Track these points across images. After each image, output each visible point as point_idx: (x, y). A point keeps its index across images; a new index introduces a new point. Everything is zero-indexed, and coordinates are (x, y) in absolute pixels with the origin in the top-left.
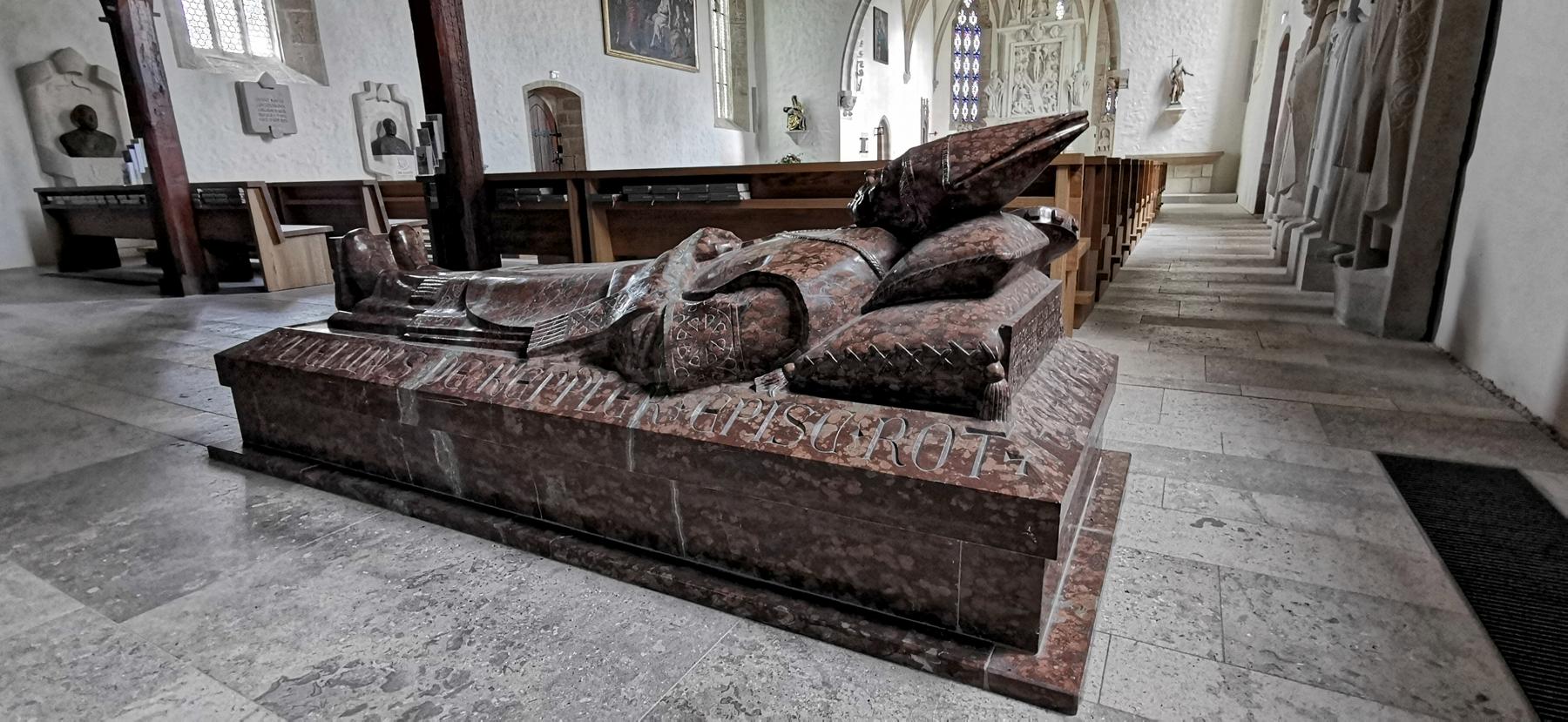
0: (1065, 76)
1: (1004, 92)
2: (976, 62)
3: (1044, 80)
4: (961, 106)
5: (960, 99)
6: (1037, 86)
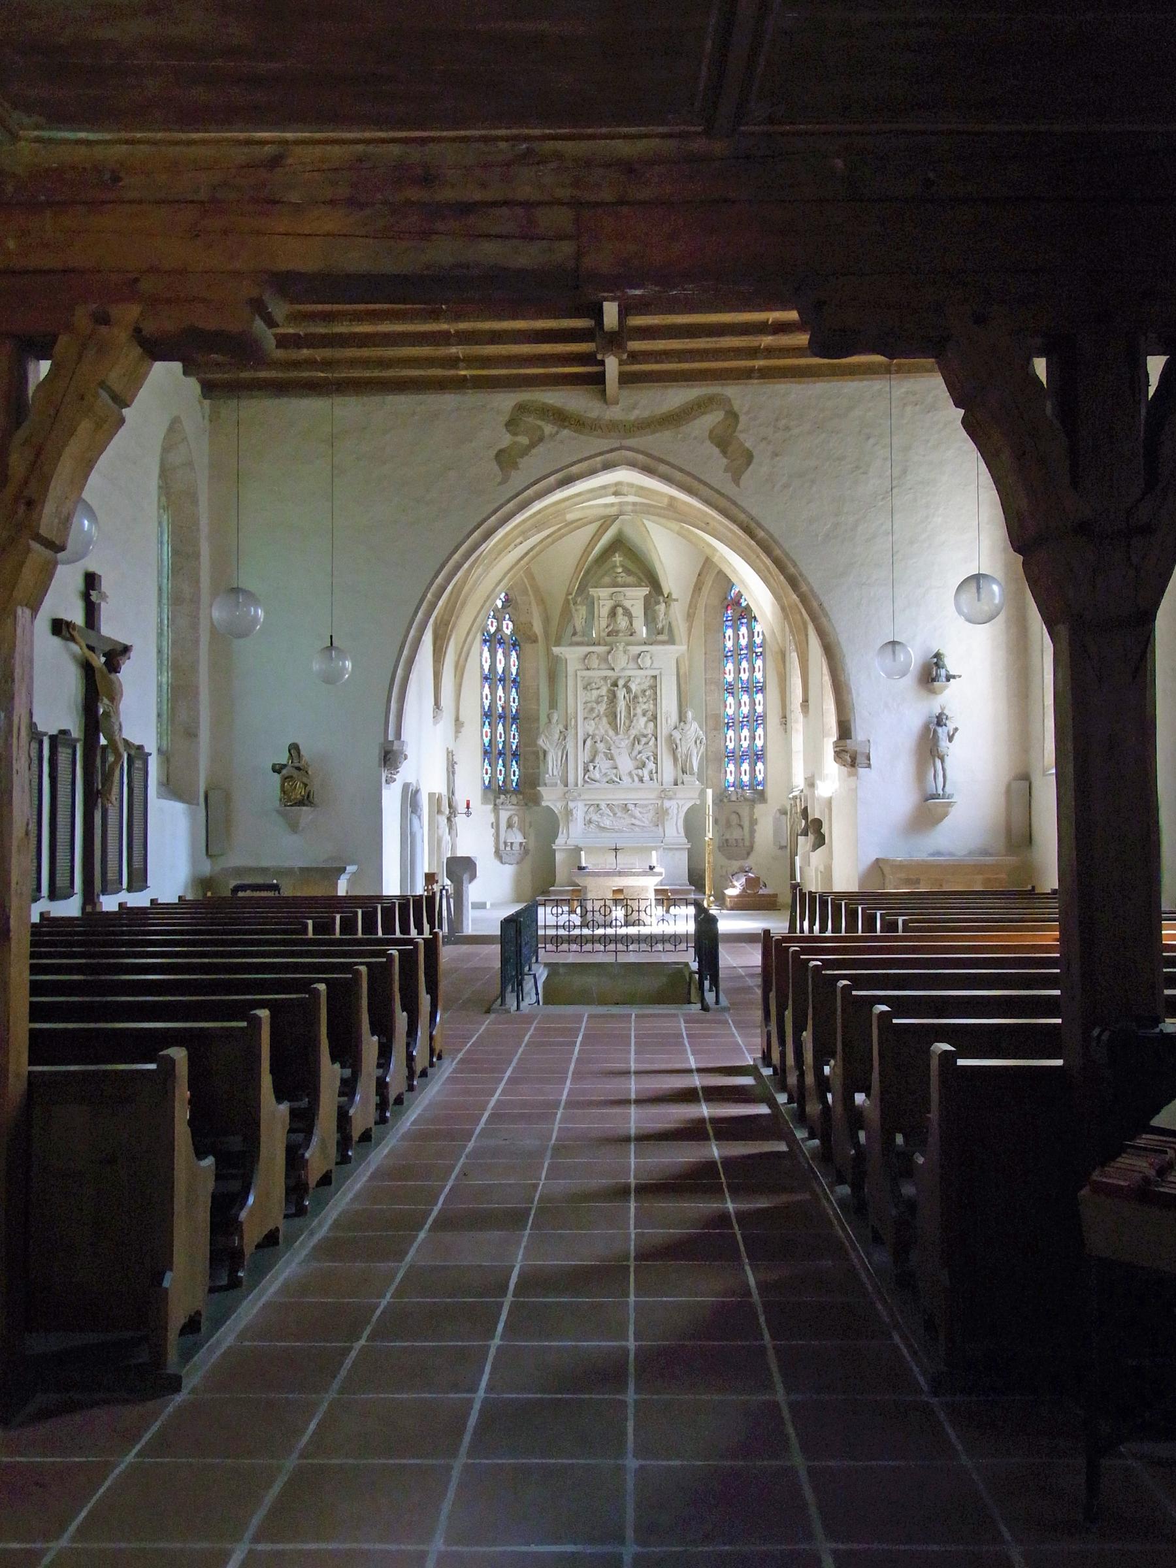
0: (663, 731)
2: (514, 693)
3: (633, 732)
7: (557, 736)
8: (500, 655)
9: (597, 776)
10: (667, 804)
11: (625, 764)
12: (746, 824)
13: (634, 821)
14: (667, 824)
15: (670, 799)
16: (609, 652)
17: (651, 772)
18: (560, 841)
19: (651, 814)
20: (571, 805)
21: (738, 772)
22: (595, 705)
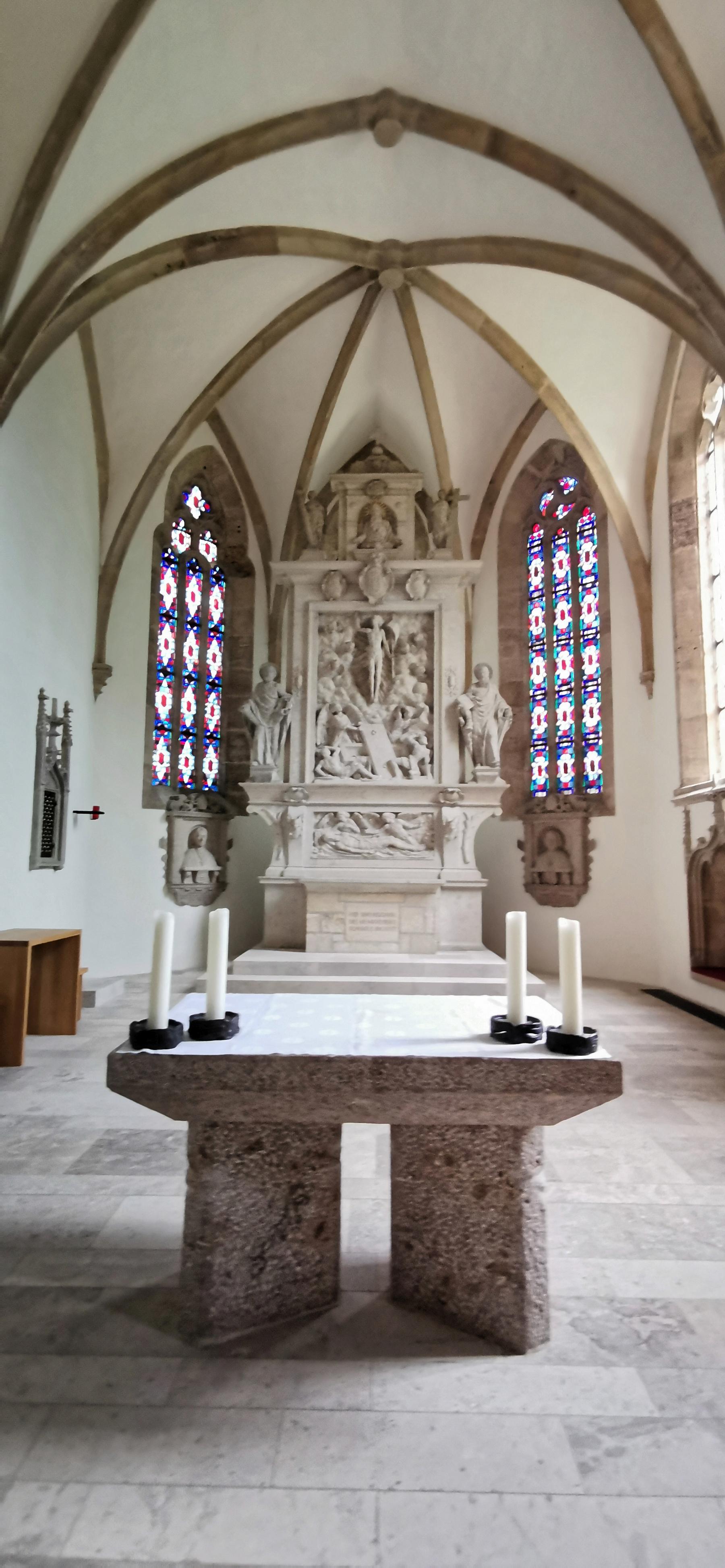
1: (293, 718)
3: (395, 698)
4: (175, 749)
5: (176, 732)
6: (377, 712)
7: (273, 702)
8: (193, 586)
9: (338, 766)
10: (448, 813)
11: (382, 748)
12: (575, 846)
13: (393, 840)
14: (447, 848)
15: (453, 806)
16: (359, 572)
17: (422, 762)
18: (274, 870)
19: (422, 830)
20: (293, 812)
21: (552, 769)
22: (335, 657)
